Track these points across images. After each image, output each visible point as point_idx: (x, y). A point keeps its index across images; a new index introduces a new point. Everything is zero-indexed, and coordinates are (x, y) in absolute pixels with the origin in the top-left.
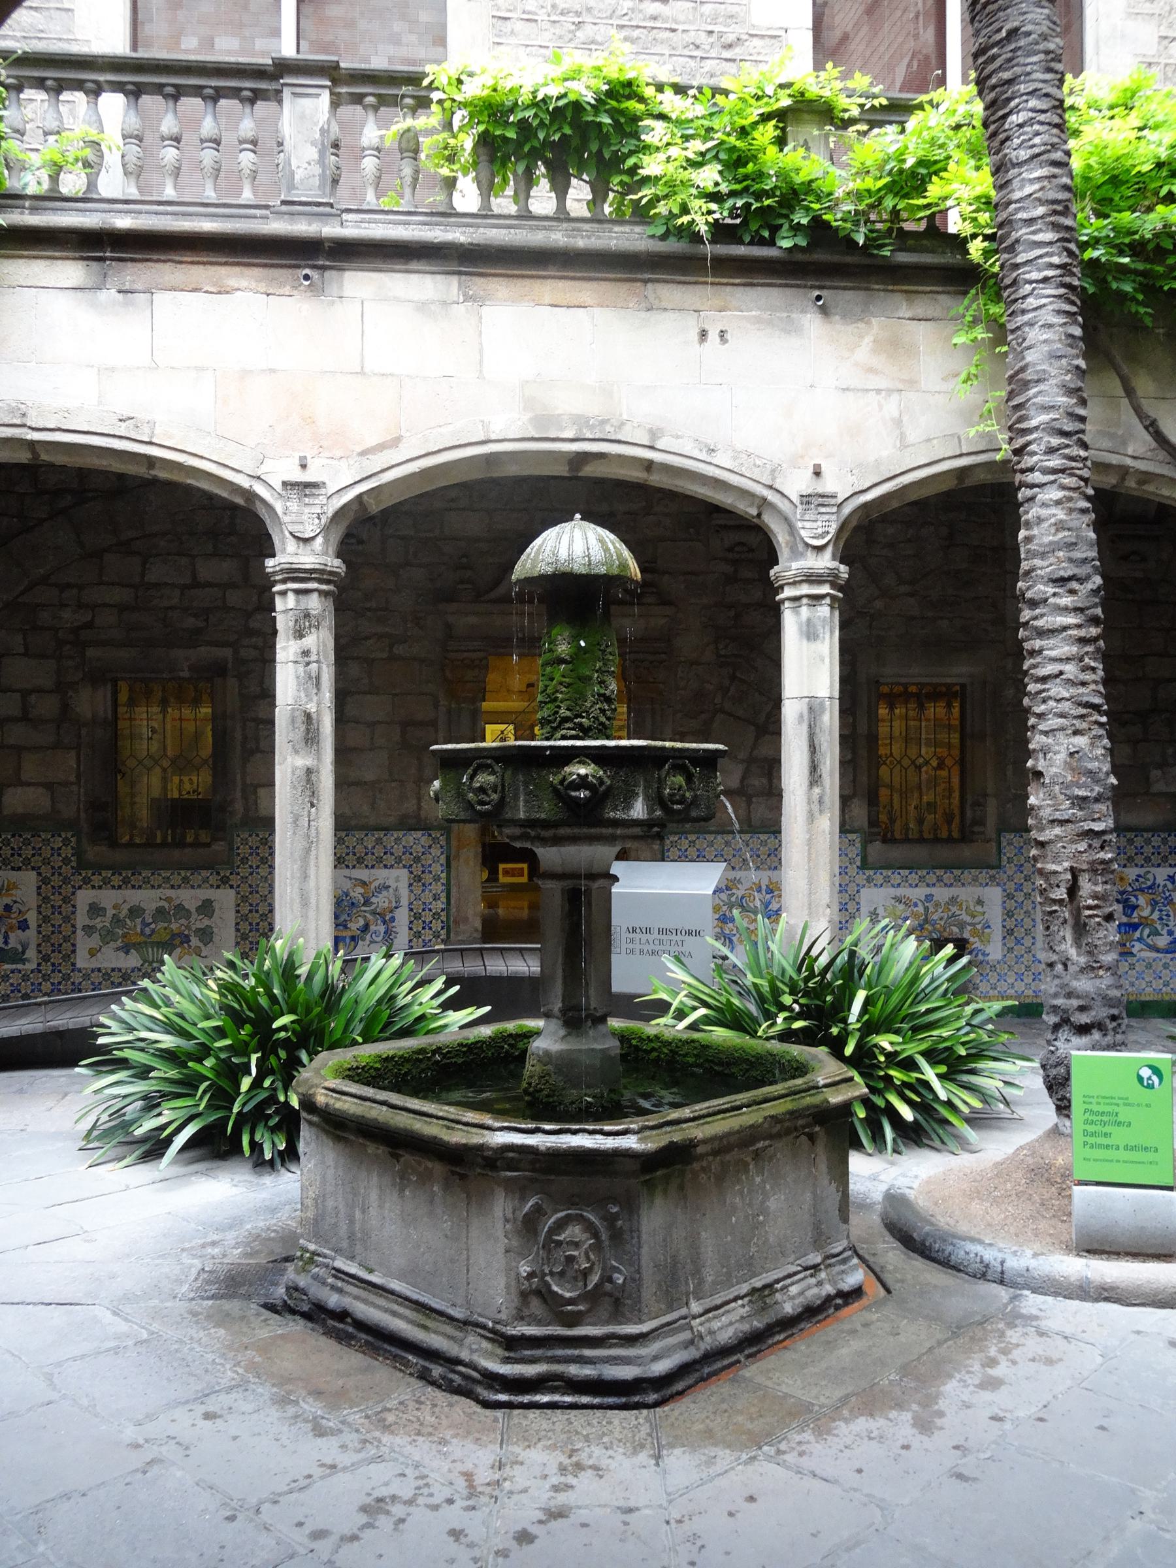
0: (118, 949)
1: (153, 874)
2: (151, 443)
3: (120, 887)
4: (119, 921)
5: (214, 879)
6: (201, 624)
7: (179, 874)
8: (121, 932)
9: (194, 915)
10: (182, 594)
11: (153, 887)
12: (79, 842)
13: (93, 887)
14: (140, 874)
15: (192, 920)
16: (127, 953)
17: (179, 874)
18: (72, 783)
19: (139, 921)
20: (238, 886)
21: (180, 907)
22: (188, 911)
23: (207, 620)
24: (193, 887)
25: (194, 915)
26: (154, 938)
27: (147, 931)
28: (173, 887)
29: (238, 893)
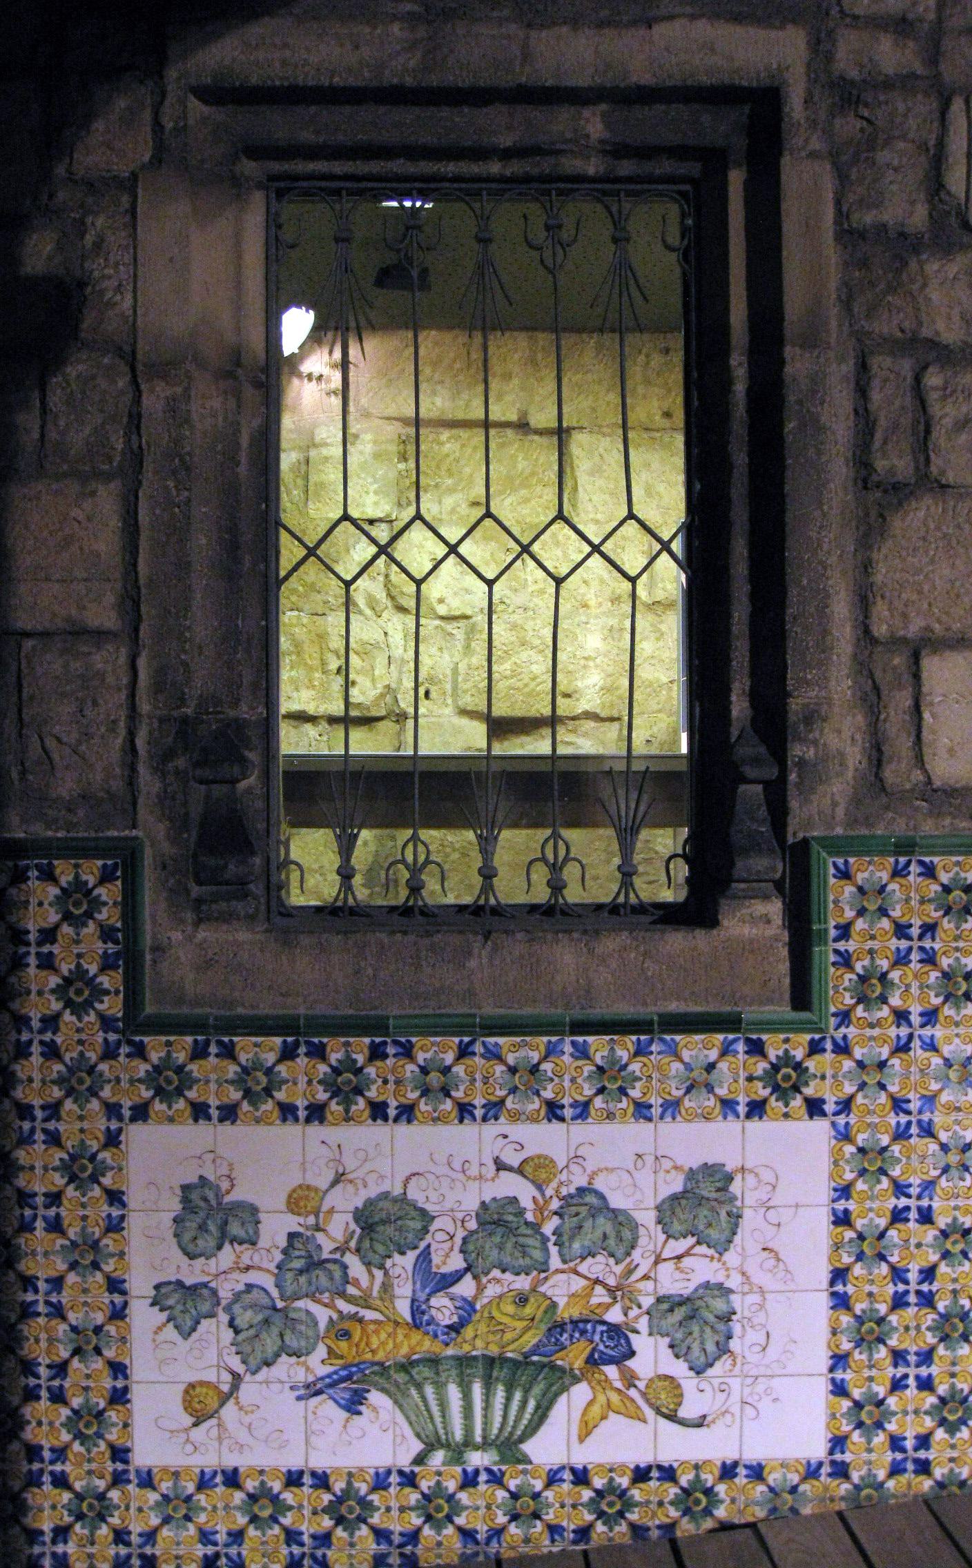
0: (313, 1390)
1: (464, 1052)
3: (317, 1113)
4: (314, 1264)
7: (582, 1053)
8: (323, 1315)
9: (651, 1235)
11: (464, 1111)
12: (130, 905)
13: (199, 1111)
14: (407, 1052)
15: (642, 1258)
16: (354, 1404)
17: (582, 1053)
18: (100, 636)
19: (404, 1263)
20: (846, 1105)
22: (621, 1220)
24: (642, 1110)
25: (651, 1235)
26: (477, 1341)
27: (443, 1309)
28: (553, 1111)
29: (845, 1136)
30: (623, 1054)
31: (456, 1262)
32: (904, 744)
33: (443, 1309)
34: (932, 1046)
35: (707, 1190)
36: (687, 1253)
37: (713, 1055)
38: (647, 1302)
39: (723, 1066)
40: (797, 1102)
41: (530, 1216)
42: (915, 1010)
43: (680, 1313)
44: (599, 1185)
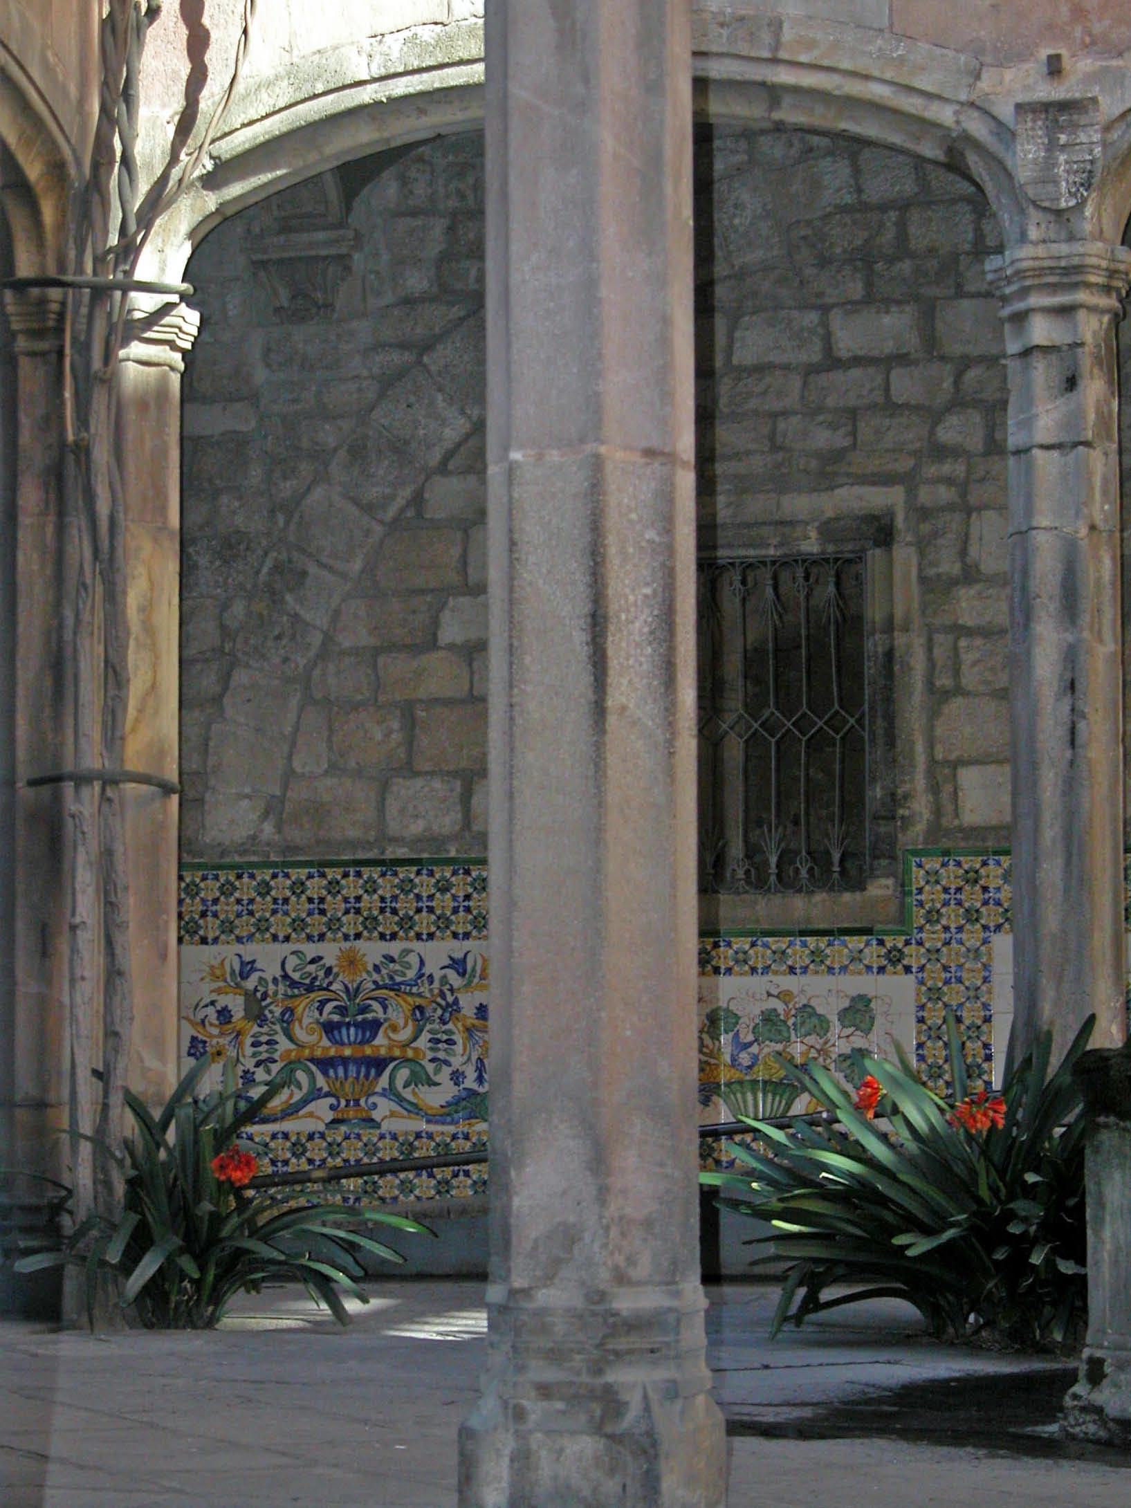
1: (753, 945)
2: (775, 61)
5: (873, 954)
6: (840, 440)
7: (804, 945)
9: (836, 1027)
10: (805, 383)
11: (753, 970)
14: (729, 945)
20: (922, 969)
21: (807, 1010)
23: (854, 434)
24: (830, 970)
25: (836, 1027)
27: (744, 1058)
28: (792, 970)
29: (922, 982)
30: (822, 946)
31: (750, 1038)
32: (949, 808)
33: (744, 1058)
34: (961, 942)
35: (860, 1006)
36: (852, 1034)
37: (862, 946)
38: (834, 1056)
39: (866, 950)
40: (900, 967)
41: (782, 1017)
42: (953, 926)
43: (848, 1062)
44: (813, 1003)
